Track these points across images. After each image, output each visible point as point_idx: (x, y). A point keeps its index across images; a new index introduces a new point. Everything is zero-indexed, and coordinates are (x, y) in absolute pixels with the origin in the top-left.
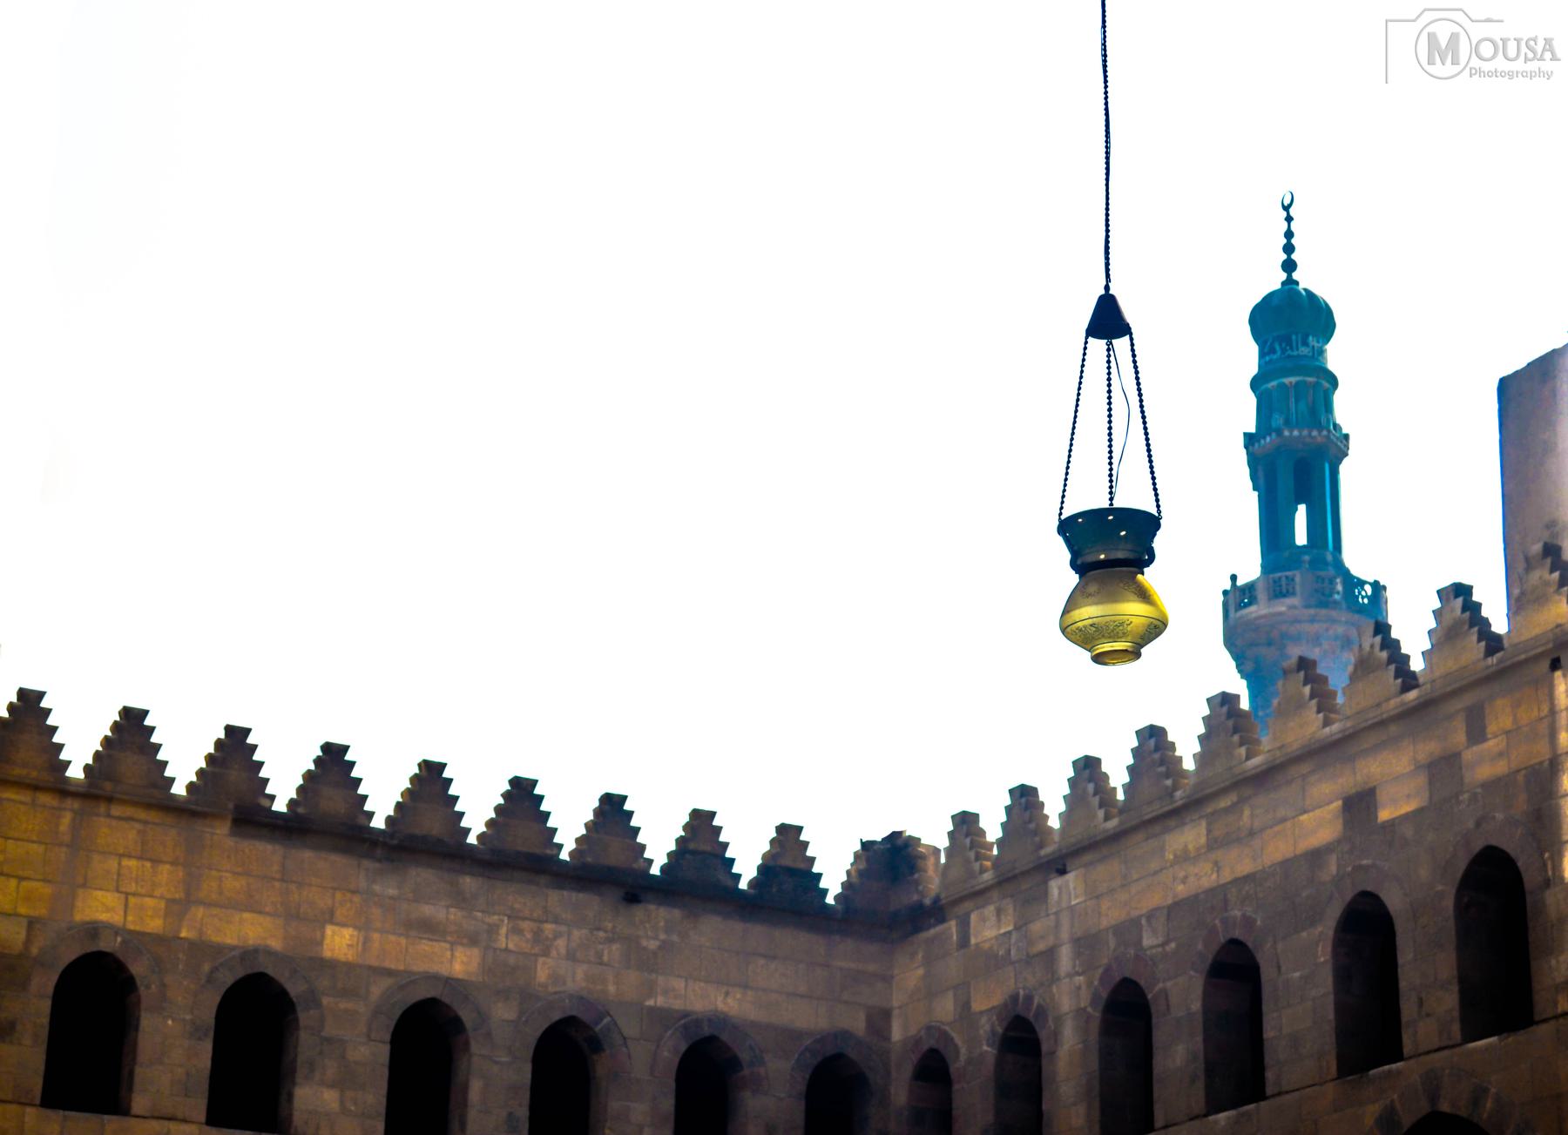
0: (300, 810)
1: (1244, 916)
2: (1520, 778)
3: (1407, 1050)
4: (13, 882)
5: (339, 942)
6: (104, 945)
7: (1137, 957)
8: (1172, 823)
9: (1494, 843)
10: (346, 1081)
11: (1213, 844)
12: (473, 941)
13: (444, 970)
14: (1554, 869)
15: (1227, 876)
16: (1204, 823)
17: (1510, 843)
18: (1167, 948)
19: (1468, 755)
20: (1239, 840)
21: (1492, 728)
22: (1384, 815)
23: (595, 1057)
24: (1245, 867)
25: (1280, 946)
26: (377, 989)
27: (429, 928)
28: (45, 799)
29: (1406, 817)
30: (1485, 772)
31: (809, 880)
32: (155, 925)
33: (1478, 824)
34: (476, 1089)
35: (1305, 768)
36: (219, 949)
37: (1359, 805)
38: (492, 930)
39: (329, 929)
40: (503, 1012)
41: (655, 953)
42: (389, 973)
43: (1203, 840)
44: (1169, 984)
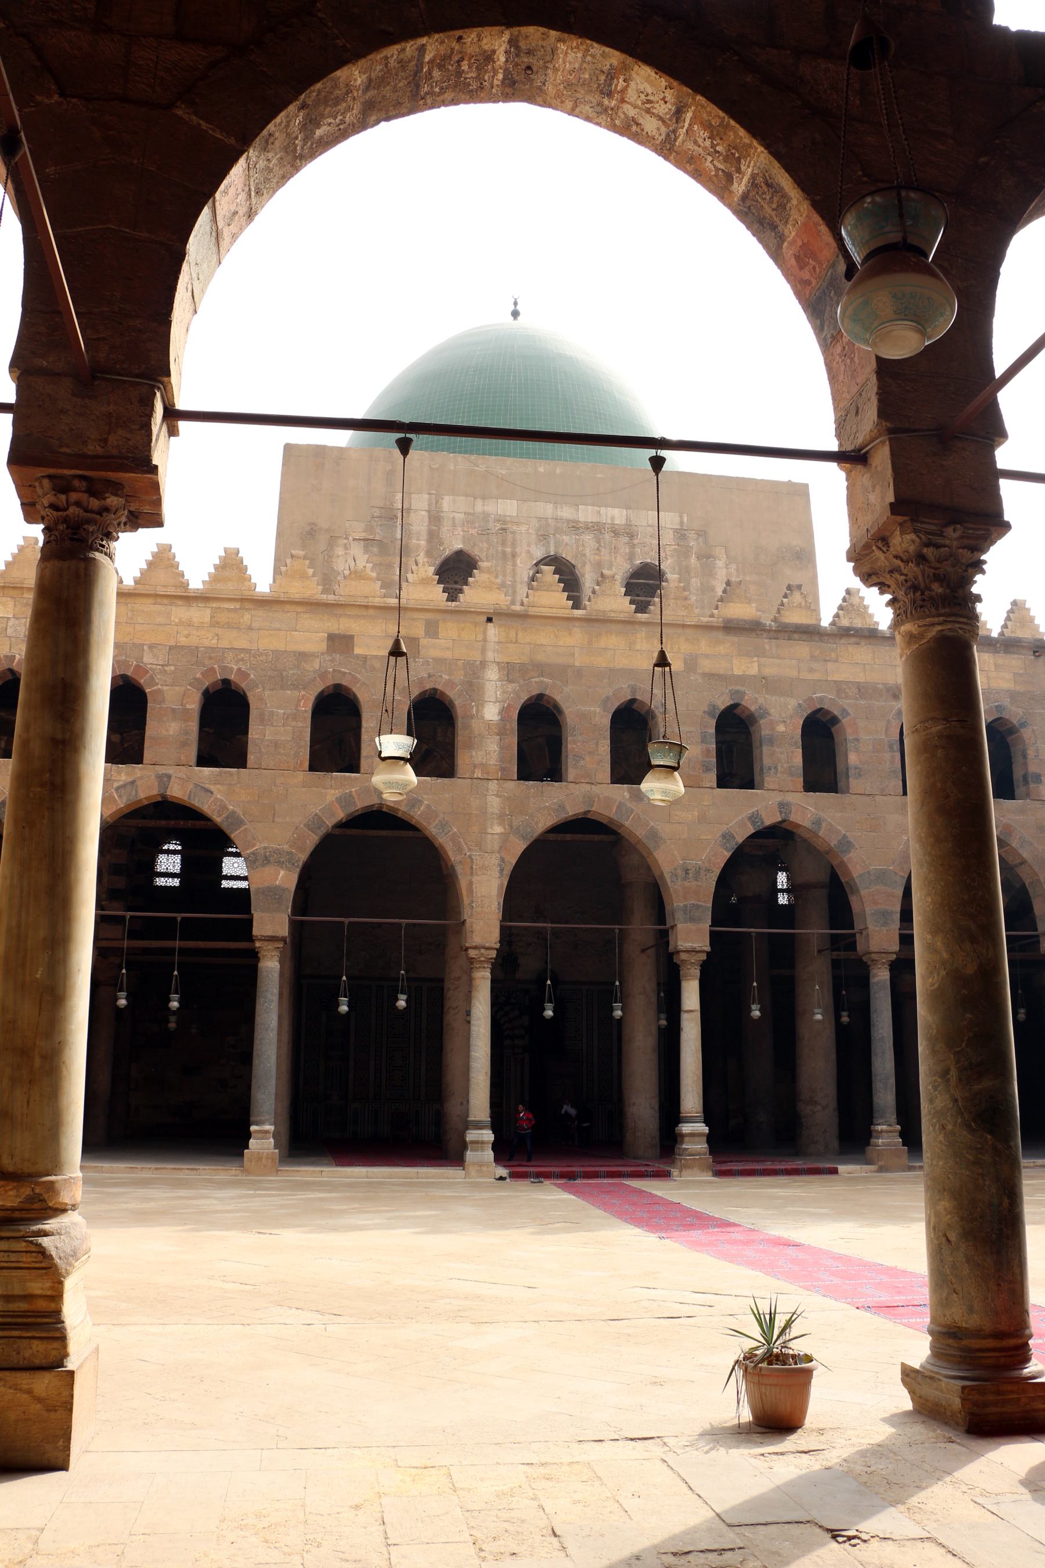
1: (239, 669)
2: (460, 663)
3: (362, 771)
7: (138, 666)
8: (180, 602)
9: (440, 687)
11: (214, 624)
14: (477, 712)
15: (224, 644)
16: (208, 611)
17: (452, 694)
18: (166, 668)
19: (424, 642)
20: (238, 628)
21: (440, 635)
22: (357, 651)
24: (242, 643)
25: (267, 693)
29: (376, 657)
30: (434, 653)
33: (430, 676)
35: (299, 609)
37: (341, 643)
43: (207, 619)
44: (165, 688)
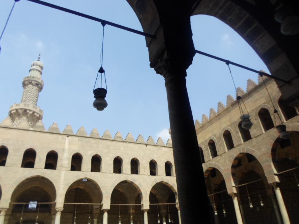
6: (225, 130)
26: (254, 113)
32: (229, 124)
36: (235, 122)
42: (255, 109)
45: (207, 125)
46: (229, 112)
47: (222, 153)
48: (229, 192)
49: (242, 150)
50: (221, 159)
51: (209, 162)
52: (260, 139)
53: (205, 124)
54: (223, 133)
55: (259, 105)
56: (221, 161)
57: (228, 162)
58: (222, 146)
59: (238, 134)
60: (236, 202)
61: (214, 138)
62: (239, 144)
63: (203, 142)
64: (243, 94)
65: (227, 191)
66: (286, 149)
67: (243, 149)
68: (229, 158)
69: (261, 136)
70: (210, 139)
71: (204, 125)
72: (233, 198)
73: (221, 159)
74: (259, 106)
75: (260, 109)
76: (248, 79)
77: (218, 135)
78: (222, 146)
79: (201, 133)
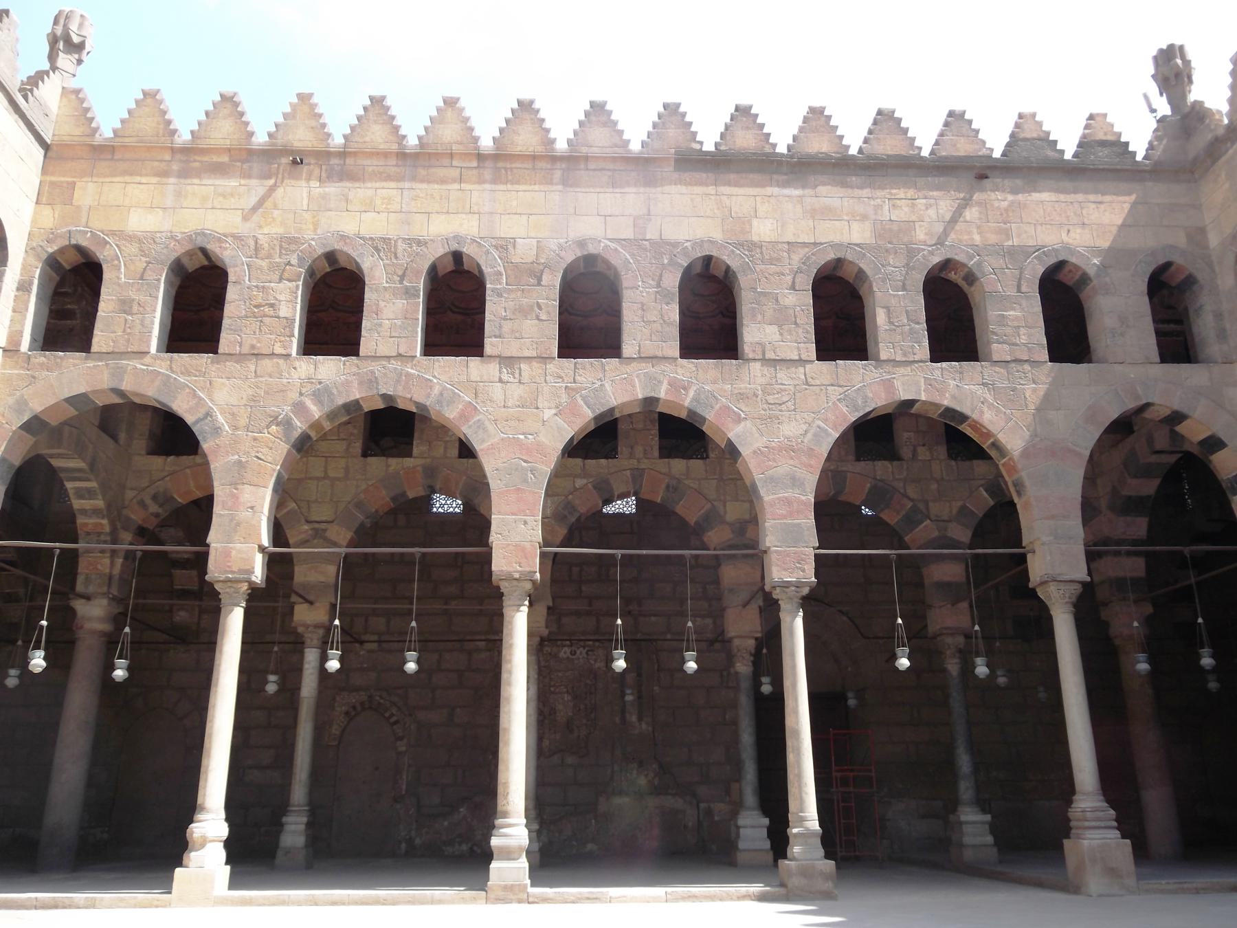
0: (723, 148)
4: (525, 218)
5: (763, 230)
6: (592, 249)
10: (782, 319)
12: (864, 218)
13: (845, 239)
23: (973, 289)
26: (796, 258)
27: (827, 213)
28: (542, 164)
31: (1122, 148)
32: (628, 234)
34: (881, 317)
36: (675, 245)
38: (878, 208)
39: (755, 222)
40: (894, 265)
41: (1006, 210)
42: (804, 244)
45: (455, 163)
46: (650, 182)
47: (527, 353)
48: (502, 563)
49: (665, 386)
50: (501, 381)
51: (395, 365)
52: (783, 375)
53: (451, 156)
54: (570, 257)
55: (837, 238)
56: (497, 391)
57: (548, 414)
58: (538, 318)
59: (667, 304)
60: (519, 628)
61: (488, 252)
62: (660, 354)
63: (384, 240)
64: (768, 149)
65: (487, 559)
66: (678, 465)
67: (674, 385)
68: (564, 398)
69: (801, 369)
70: (455, 246)
71: (437, 156)
72: (507, 602)
73: (501, 381)
74: (834, 246)
75: (831, 256)
76: (377, 93)
77: (524, 252)
78: (538, 318)
79: (393, 184)
